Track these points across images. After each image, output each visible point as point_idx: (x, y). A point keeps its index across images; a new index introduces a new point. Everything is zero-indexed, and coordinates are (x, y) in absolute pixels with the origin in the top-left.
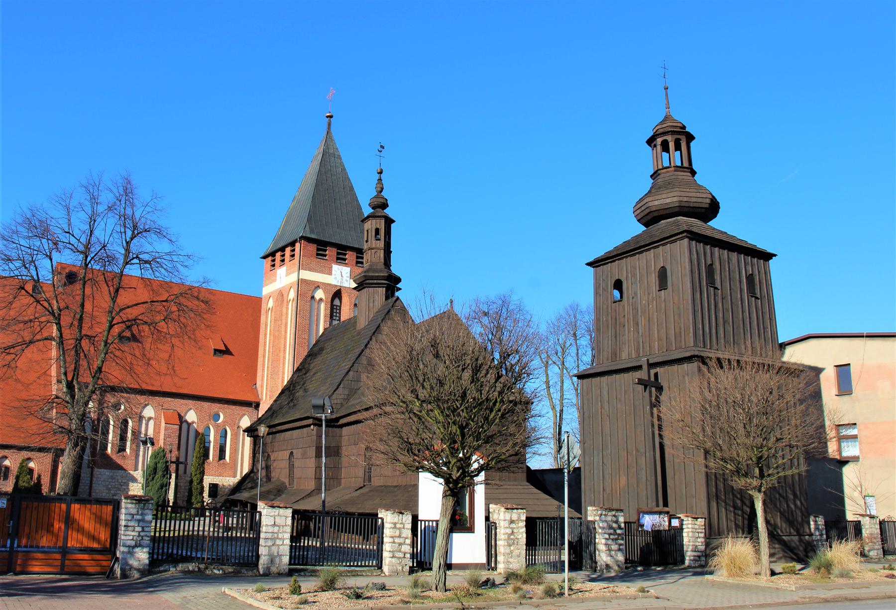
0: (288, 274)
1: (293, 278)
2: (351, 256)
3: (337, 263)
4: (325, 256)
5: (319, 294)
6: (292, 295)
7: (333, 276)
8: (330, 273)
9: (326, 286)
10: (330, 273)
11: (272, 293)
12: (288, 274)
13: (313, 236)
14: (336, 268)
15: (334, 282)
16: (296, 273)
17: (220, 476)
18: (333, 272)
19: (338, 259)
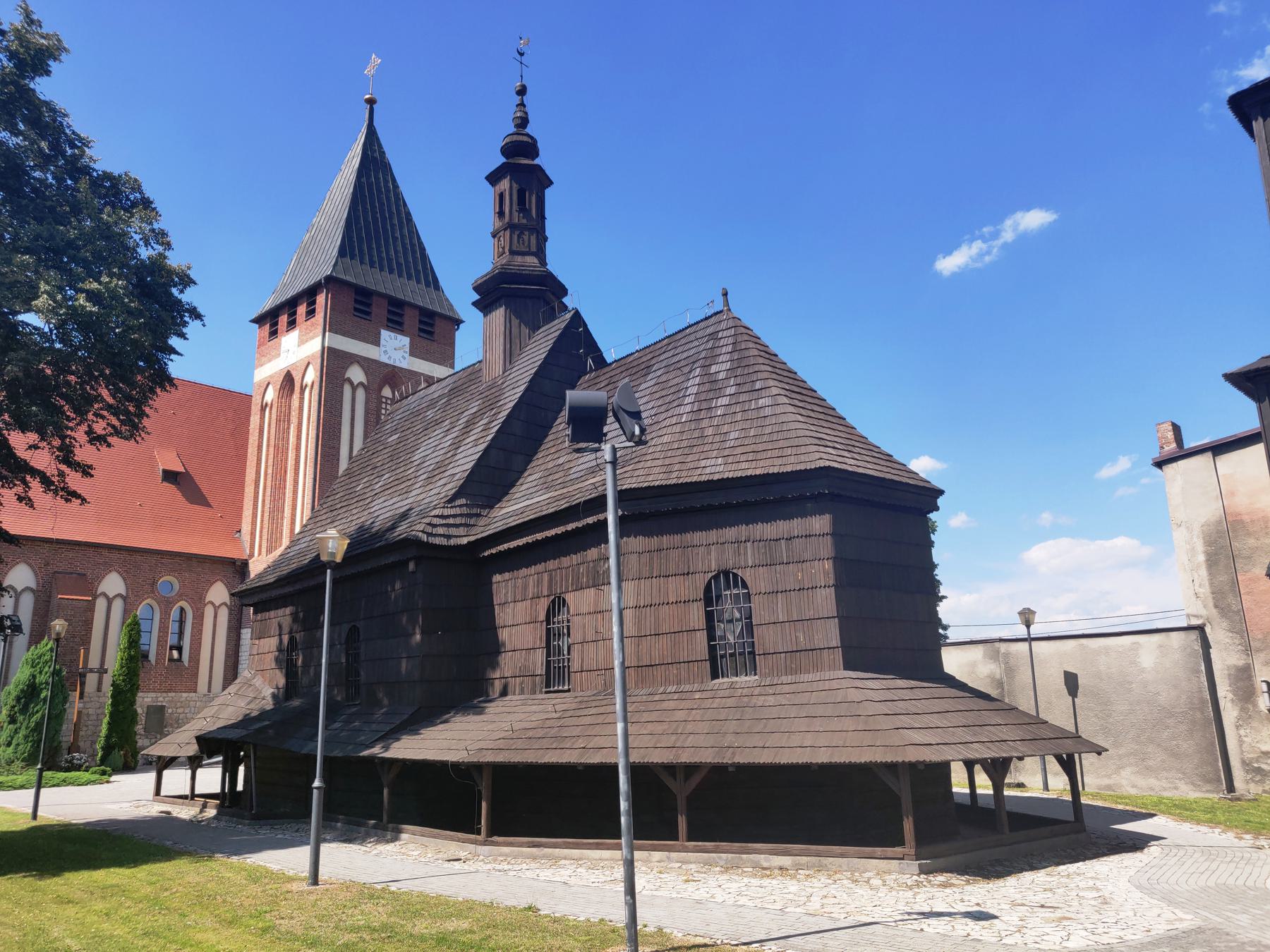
0: (302, 342)
1: (314, 346)
2: (411, 318)
3: (388, 328)
4: (368, 314)
5: (356, 374)
6: (312, 375)
7: (383, 349)
8: (377, 343)
9: (368, 365)
10: (377, 343)
11: (271, 377)
12: (302, 342)
13: (348, 278)
14: (385, 334)
15: (384, 359)
16: (320, 338)
17: (170, 691)
18: (382, 342)
19: (389, 320)
